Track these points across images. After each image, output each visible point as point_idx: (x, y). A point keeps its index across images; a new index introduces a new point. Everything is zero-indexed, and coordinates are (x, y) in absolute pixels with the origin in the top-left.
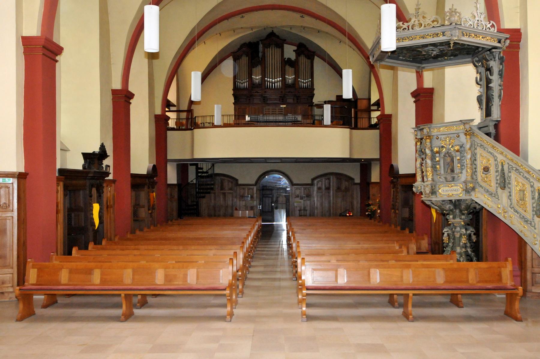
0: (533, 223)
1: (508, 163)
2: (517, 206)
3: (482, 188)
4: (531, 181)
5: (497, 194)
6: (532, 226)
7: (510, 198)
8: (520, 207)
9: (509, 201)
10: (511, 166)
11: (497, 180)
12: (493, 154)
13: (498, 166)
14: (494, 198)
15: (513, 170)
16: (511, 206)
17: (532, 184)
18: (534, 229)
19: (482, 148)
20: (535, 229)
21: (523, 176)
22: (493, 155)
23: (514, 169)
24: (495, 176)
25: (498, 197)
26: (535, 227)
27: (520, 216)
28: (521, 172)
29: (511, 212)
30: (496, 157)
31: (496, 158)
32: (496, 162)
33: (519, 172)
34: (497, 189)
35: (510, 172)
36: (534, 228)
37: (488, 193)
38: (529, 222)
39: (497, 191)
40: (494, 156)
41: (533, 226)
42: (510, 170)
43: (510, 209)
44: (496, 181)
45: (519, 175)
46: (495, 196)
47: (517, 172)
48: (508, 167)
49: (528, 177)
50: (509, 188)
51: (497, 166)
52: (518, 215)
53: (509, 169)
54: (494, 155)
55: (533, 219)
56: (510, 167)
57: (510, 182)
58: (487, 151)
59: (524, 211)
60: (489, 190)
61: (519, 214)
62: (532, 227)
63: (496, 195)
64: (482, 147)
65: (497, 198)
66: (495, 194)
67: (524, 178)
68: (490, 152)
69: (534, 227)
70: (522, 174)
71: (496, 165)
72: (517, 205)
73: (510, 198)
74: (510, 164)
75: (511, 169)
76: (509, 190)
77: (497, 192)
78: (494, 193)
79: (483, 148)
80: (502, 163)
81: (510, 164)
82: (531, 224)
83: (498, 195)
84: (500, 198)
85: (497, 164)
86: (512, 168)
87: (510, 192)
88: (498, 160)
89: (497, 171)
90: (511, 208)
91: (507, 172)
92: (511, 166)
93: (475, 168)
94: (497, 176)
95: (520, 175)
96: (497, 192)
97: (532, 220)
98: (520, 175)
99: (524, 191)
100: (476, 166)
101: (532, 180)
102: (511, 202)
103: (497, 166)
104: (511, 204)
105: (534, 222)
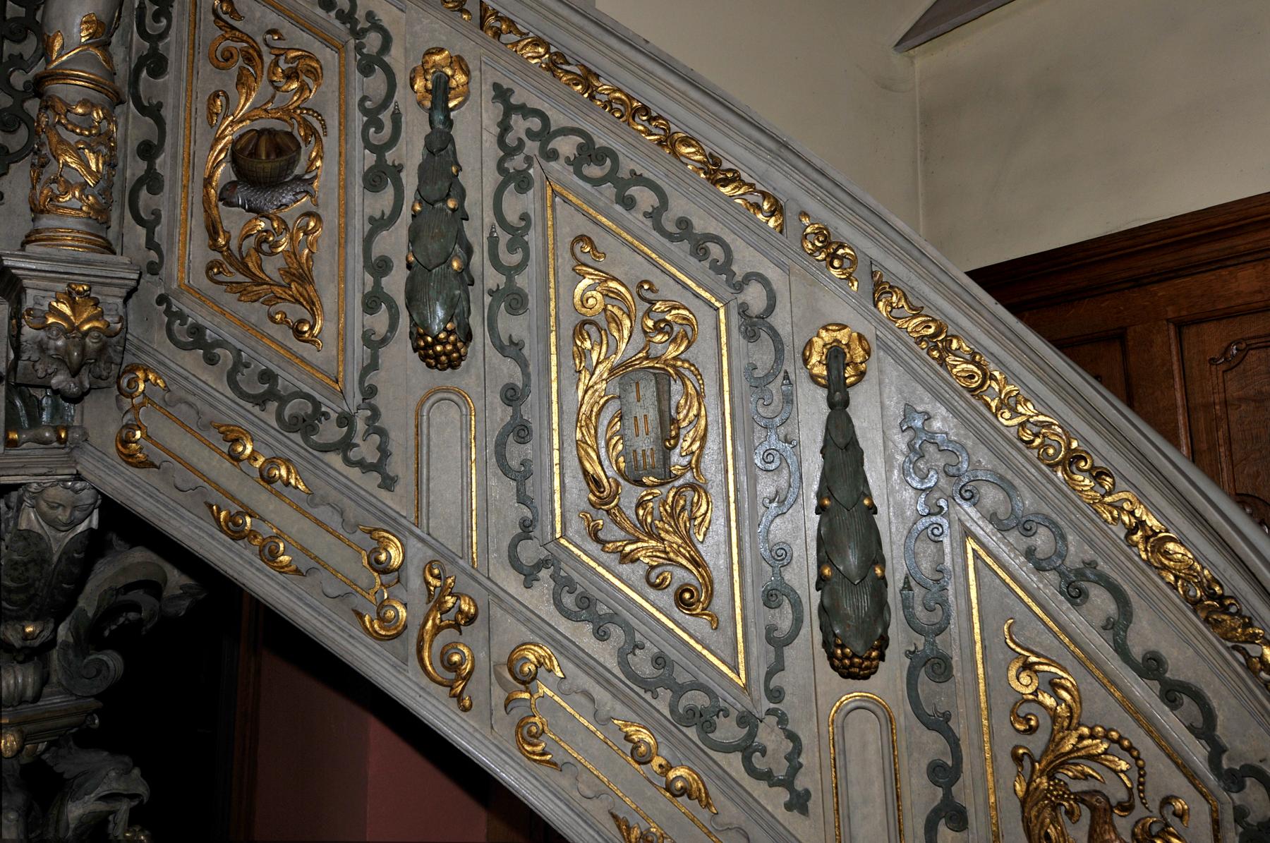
0: (769, 736)
2: (593, 547)
3: (211, 360)
5: (376, 413)
6: (767, 777)
7: (516, 453)
8: (626, 558)
9: (502, 489)
10: (535, 124)
11: (380, 267)
13: (396, 118)
14: (335, 459)
15: (553, 155)
17: (755, 297)
18: (781, 814)
20: (799, 803)
21: (655, 216)
23: (567, 146)
25: (384, 452)
26: (801, 783)
28: (638, 179)
30: (377, 27)
31: (373, 42)
32: (376, 84)
33: (611, 177)
35: (523, 182)
37: (273, 406)
38: (727, 730)
39: (371, 379)
41: (781, 771)
42: (517, 162)
43: (511, 583)
44: (369, 279)
45: (618, 208)
46: (344, 446)
47: (596, 182)
48: (505, 127)
49: (702, 224)
50: (511, 349)
51: (380, 127)
52: (605, 654)
54: (360, 14)
55: (776, 695)
56: (520, 125)
57: (521, 281)
59: (667, 598)
60: (288, 379)
62: (758, 789)
63: (360, 426)
66: (346, 420)
67: (671, 237)
69: (788, 783)
70: (645, 198)
72: (594, 534)
73: (516, 453)
75: (532, 147)
76: (508, 371)
77: (378, 401)
78: (331, 407)
80: (441, 90)
82: (747, 749)
83: (382, 432)
85: (384, 105)
86: (545, 134)
87: (512, 396)
90: (529, 577)
91: (492, 178)
92: (535, 124)
93: (148, 151)
94: (379, 224)
95: (629, 203)
96: (370, 392)
97: (767, 705)
98: (629, 203)
99: (663, 377)
100: (160, 122)
102: (523, 499)
104: (526, 529)
105: (782, 720)
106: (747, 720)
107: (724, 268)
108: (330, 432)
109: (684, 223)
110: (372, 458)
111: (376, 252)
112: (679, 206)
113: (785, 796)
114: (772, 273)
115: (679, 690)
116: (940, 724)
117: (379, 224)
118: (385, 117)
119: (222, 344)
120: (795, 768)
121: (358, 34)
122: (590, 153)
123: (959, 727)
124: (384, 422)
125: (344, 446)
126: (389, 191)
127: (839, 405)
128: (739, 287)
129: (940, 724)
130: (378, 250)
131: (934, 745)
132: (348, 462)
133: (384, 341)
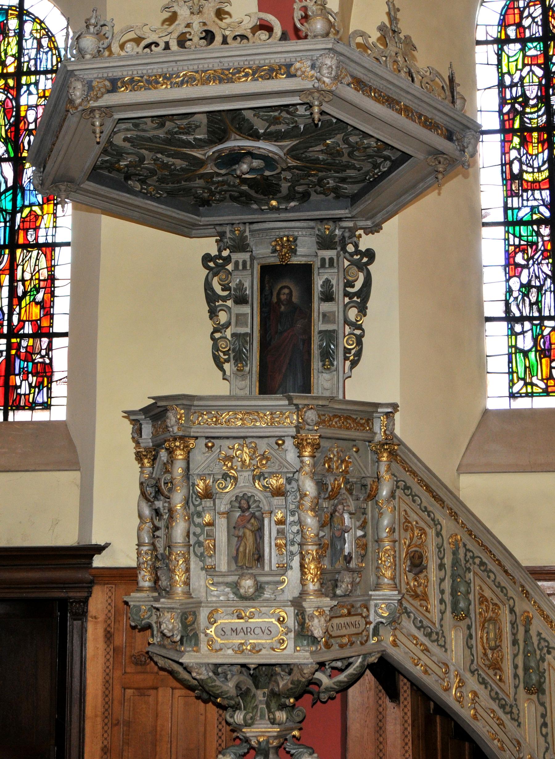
0: (515, 710)
1: (465, 545)
4: (509, 595)
5: (443, 633)
10: (471, 554)
12: (432, 515)
13: (444, 550)
15: (474, 563)
16: (474, 667)
19: (408, 495)
21: (494, 581)
22: (433, 520)
23: (477, 561)
24: (439, 581)
25: (445, 642)
27: (490, 692)
28: (491, 571)
29: (472, 683)
32: (440, 540)
34: (442, 619)
36: (516, 723)
40: (436, 523)
42: (468, 565)
43: (468, 675)
47: (483, 571)
48: (466, 555)
49: (503, 584)
53: (467, 561)
56: (469, 554)
58: (420, 505)
61: (489, 688)
64: (406, 491)
65: (441, 646)
68: (425, 508)
69: (517, 720)
70: (492, 575)
71: (440, 547)
74: (467, 547)
75: (471, 561)
79: (411, 494)
81: (467, 547)
82: (511, 713)
83: (444, 637)
84: (447, 646)
86: (473, 558)
87: (469, 627)
88: (444, 532)
89: (441, 566)
90: (472, 672)
101: (511, 593)
103: (442, 549)
104: (472, 661)
106: (511, 706)
107: (506, 595)
108: (434, 637)
109: (499, 583)
110: (443, 644)
111: (442, 587)
112: (498, 579)
113: (516, 723)
114: (514, 597)
115: (500, 700)
116: (543, 704)
117: (442, 580)
118: (442, 549)
119: (411, 612)
120: (519, 717)
121: (436, 525)
122: (482, 564)
123: (548, 705)
124: (445, 634)
125: (437, 640)
126: (443, 571)
127: (527, 631)
128: (509, 600)
129: (543, 704)
130: (442, 587)
131: (541, 709)
132: (438, 645)
133: (444, 612)
